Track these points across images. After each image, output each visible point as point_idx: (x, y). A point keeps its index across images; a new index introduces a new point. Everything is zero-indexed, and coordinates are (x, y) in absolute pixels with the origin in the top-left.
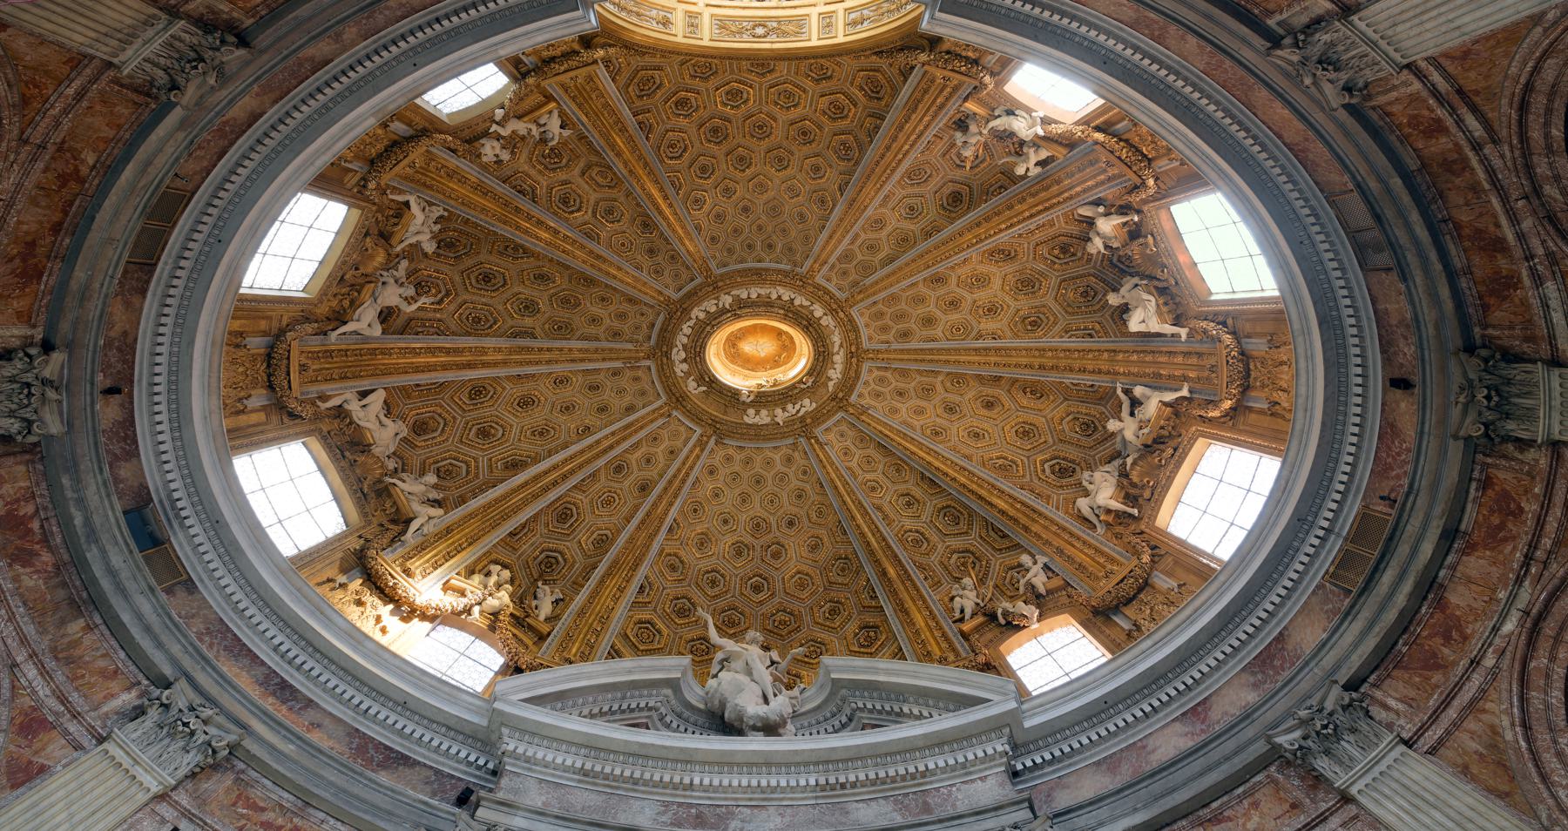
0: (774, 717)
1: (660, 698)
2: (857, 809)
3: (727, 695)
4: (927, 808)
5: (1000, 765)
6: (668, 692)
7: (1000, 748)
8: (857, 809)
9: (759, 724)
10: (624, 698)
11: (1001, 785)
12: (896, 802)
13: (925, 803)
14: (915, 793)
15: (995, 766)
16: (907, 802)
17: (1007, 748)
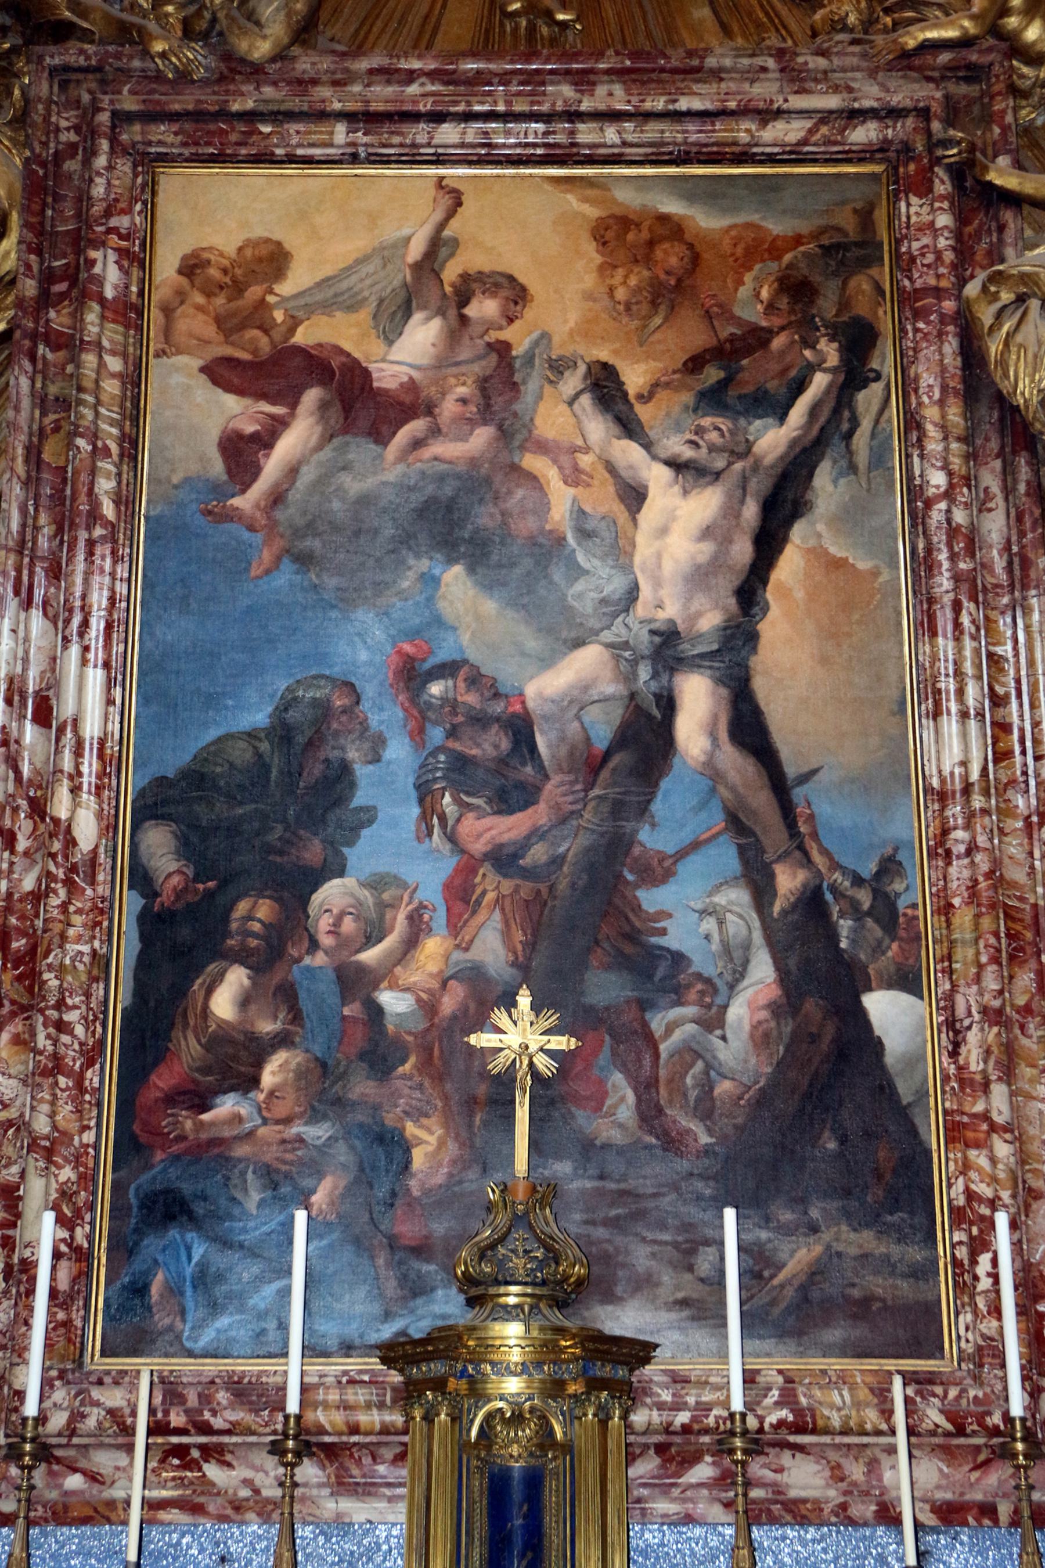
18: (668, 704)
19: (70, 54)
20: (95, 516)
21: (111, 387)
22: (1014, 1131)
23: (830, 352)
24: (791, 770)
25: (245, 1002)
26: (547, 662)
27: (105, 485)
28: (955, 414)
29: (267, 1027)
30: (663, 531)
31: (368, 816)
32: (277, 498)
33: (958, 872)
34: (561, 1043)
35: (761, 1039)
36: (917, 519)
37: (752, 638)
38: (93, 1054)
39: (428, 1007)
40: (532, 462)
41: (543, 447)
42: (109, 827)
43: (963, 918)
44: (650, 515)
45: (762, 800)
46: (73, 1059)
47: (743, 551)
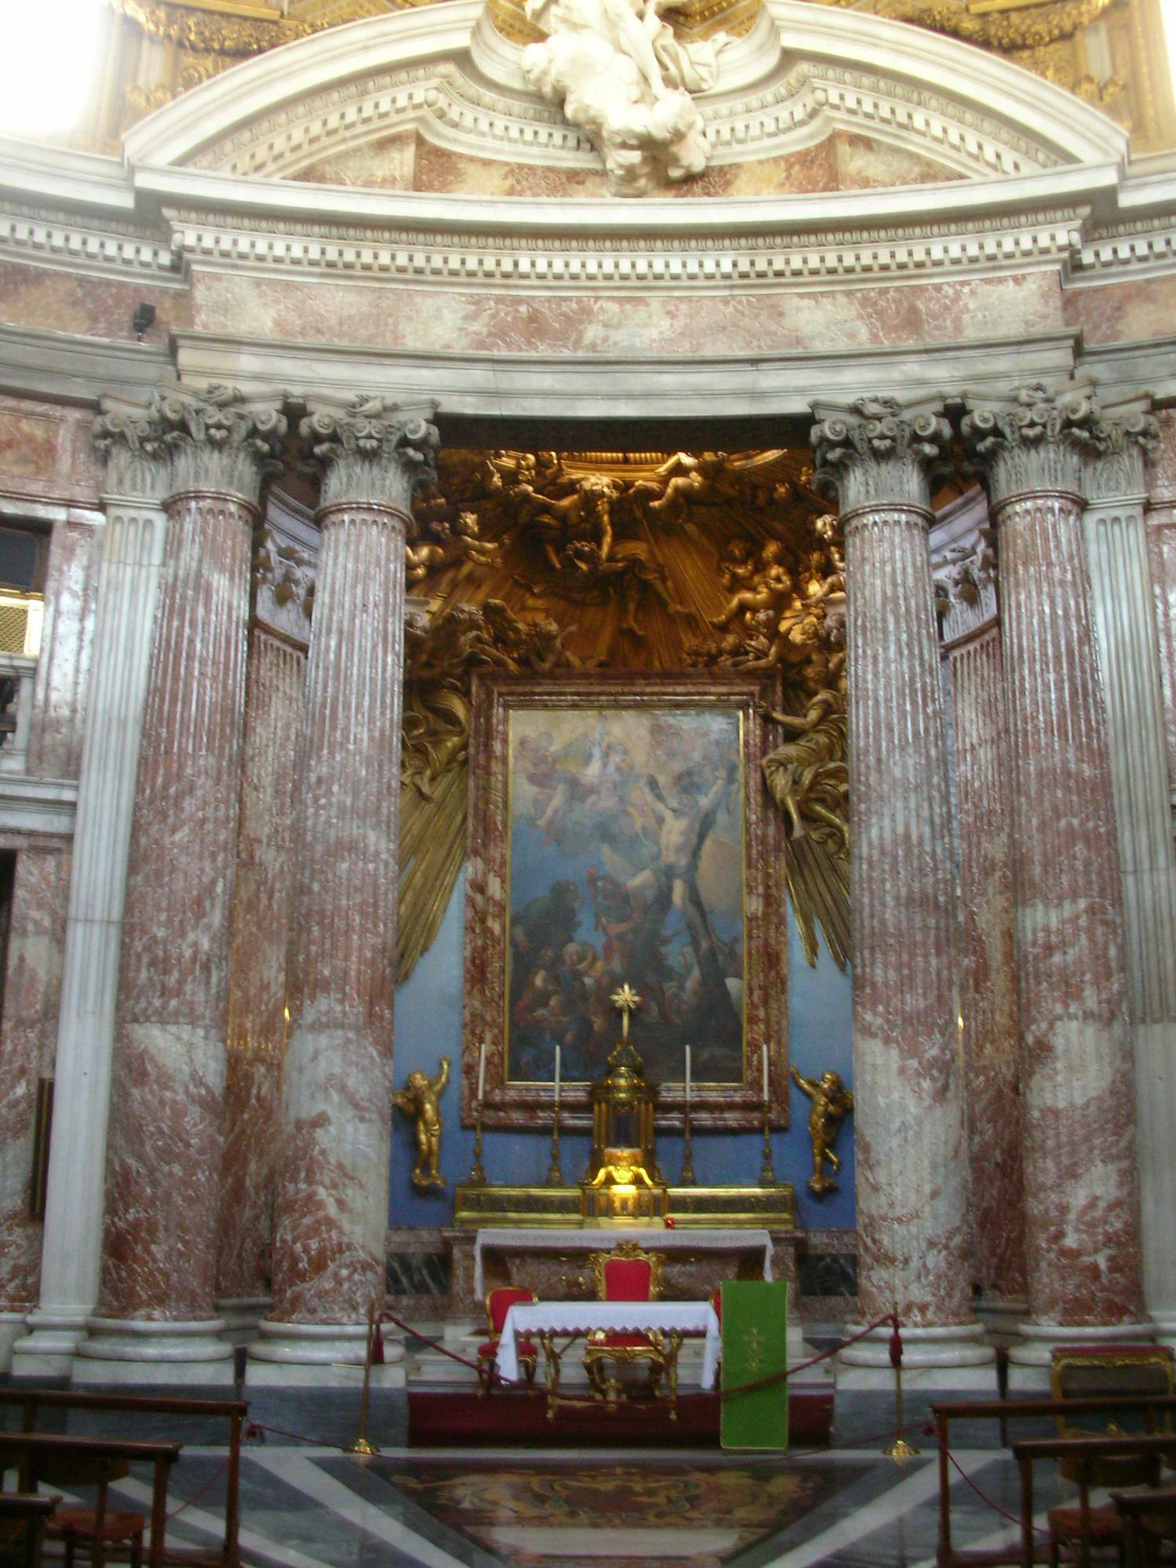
0: (660, 134)
1: (435, 82)
2: (798, 309)
3: (567, 82)
4: (912, 321)
5: (1054, 261)
6: (449, 68)
7: (1062, 239)
8: (798, 309)
9: (633, 142)
10: (364, 93)
11: (1045, 296)
12: (865, 302)
13: (913, 310)
14: (898, 289)
15: (1047, 262)
16: (882, 303)
17: (1076, 238)
18: (670, 889)
19: (484, 669)
20: (496, 829)
21: (500, 786)
22: (767, 1022)
23: (722, 773)
24: (706, 908)
25: (545, 981)
26: (634, 875)
27: (499, 818)
28: (759, 799)
29: (550, 988)
30: (669, 832)
31: (580, 924)
32: (551, 822)
33: (754, 943)
34: (637, 999)
35: (695, 993)
36: (748, 831)
37: (696, 867)
38: (502, 996)
39: (598, 982)
40: (631, 810)
41: (633, 805)
42: (503, 928)
43: (755, 957)
44: (665, 828)
45: (697, 920)
46: (496, 998)
47: (694, 839)
